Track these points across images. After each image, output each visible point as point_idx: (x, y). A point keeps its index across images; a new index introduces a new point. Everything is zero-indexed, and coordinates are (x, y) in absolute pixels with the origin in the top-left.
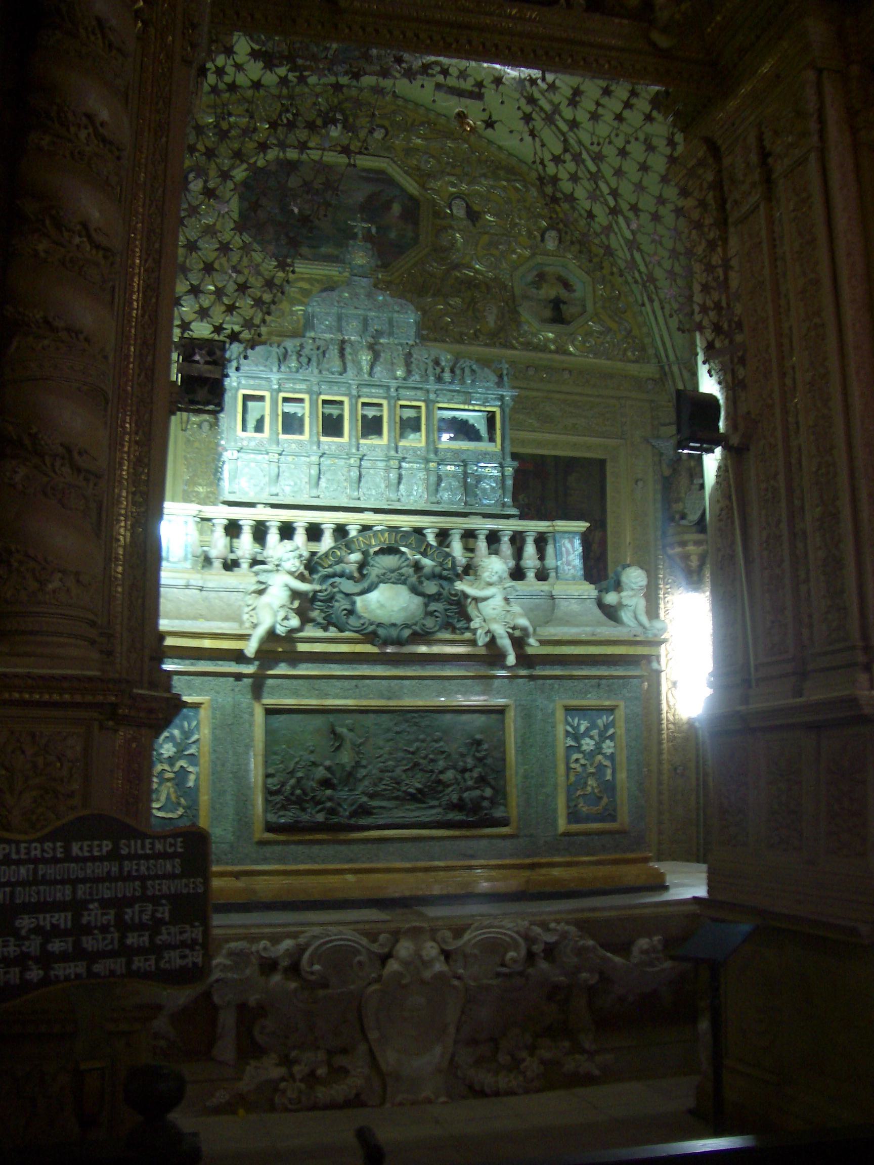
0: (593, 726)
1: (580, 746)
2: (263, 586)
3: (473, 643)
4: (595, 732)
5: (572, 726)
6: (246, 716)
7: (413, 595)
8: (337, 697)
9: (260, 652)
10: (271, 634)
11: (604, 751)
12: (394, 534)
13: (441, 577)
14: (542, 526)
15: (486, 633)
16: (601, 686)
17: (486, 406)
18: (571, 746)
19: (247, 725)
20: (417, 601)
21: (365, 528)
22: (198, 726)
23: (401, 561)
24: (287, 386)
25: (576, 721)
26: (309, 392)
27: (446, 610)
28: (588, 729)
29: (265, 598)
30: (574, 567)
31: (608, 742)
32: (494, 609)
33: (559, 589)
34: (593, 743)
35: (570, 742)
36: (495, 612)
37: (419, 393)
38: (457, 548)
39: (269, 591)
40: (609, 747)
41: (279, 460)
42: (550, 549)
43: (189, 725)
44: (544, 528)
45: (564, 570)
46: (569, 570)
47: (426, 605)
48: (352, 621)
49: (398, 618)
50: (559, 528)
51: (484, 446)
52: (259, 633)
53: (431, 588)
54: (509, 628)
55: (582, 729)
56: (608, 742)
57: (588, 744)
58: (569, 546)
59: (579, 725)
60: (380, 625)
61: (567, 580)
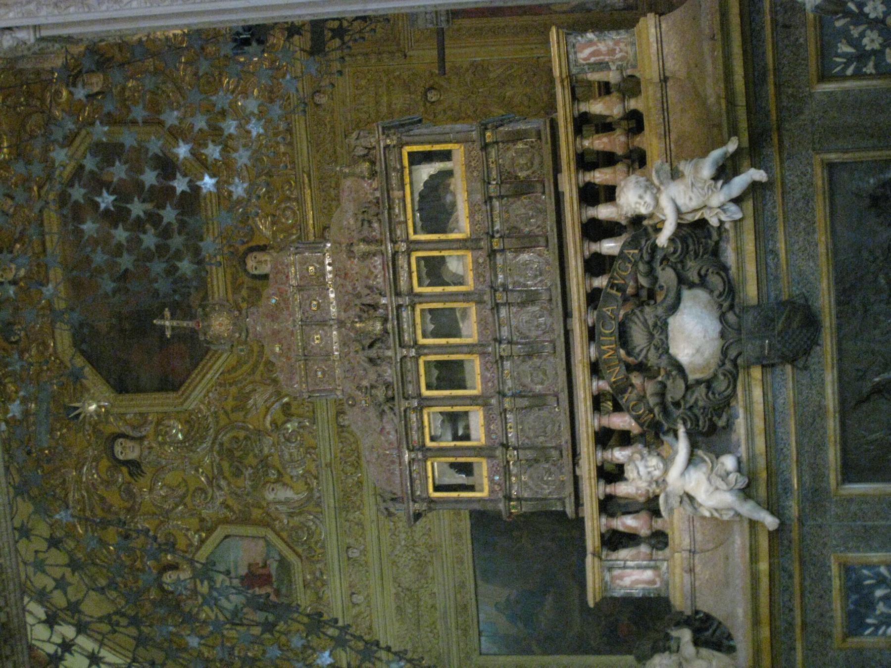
0: (845, 33)
1: (874, 52)
2: (686, 499)
3: (737, 223)
4: (855, 32)
5: (847, 65)
6: (854, 508)
7: (682, 305)
8: (822, 394)
9: (773, 508)
10: (747, 492)
11: (881, 15)
12: (602, 338)
13: (650, 263)
14: (561, 95)
15: (725, 211)
16: (787, 23)
17: (403, 167)
18: (876, 66)
19: (864, 506)
20: (686, 293)
21: (592, 334)
22: (868, 566)
23: (636, 320)
24: (415, 437)
25: (838, 60)
26: (419, 410)
27: (696, 255)
28: (851, 42)
29: (701, 496)
30: (617, 43)
31: (866, 10)
32: (691, 199)
33: (649, 72)
34: (868, 32)
35: (870, 69)
36: (694, 199)
37: (402, 261)
38: (604, 212)
39: (692, 493)
40: (875, 8)
41: (515, 448)
42: (595, 76)
43: (869, 578)
44: (566, 91)
45: (621, 59)
46: (621, 51)
47: (692, 286)
48: (721, 385)
49: (713, 327)
50: (564, 71)
51: (457, 164)
52: (748, 509)
53: (666, 276)
54: (715, 187)
55: (849, 50)
56: (866, 10)
57: (872, 41)
58: (587, 52)
59: (843, 55)
60: (724, 352)
61: (636, 54)
